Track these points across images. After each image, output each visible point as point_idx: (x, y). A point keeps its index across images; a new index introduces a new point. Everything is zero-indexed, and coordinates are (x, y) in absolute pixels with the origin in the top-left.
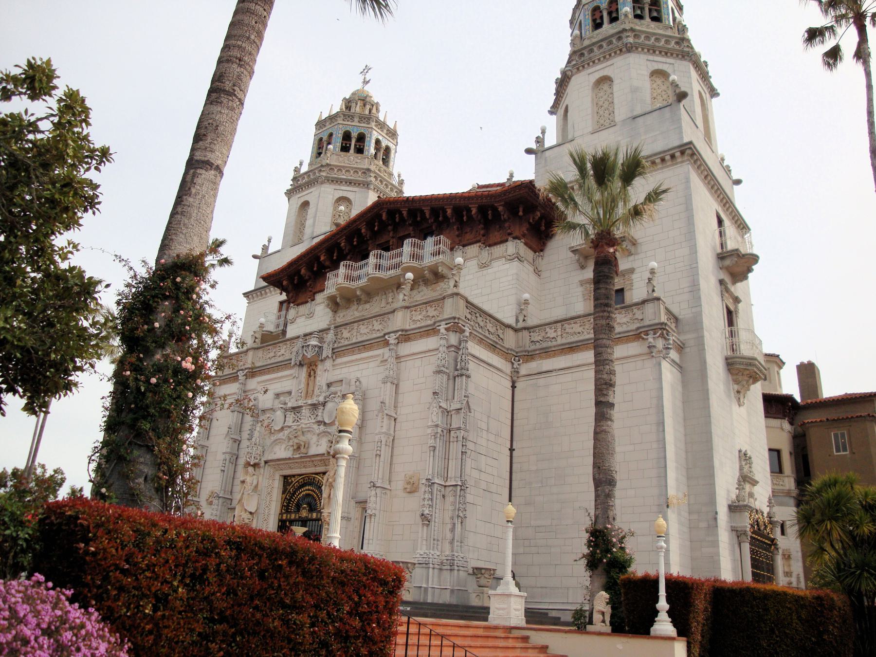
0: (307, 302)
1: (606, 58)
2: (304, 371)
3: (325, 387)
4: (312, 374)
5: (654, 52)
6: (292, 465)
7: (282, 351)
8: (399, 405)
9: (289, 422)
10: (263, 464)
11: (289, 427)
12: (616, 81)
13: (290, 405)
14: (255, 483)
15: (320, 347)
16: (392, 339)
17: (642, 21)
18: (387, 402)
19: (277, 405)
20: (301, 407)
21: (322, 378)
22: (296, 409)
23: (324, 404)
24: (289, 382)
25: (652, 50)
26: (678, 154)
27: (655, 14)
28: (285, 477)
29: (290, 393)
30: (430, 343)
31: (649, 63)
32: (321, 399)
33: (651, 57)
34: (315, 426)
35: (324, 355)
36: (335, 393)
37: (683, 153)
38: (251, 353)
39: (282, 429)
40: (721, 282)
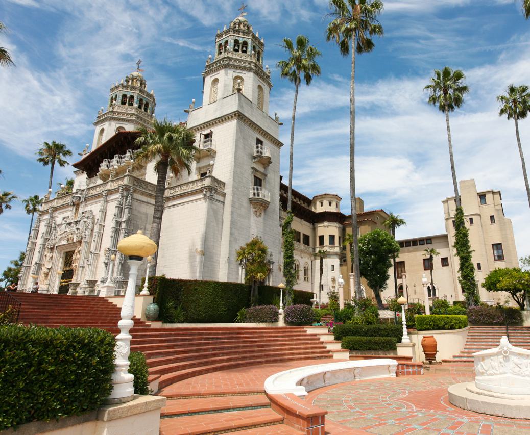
0: (93, 177)
1: (218, 69)
2: (75, 208)
3: (81, 214)
4: (77, 210)
5: (237, 68)
6: (68, 248)
7: (68, 199)
8: (106, 220)
9: (67, 229)
10: (55, 247)
11: (66, 231)
12: (219, 79)
13: (68, 222)
14: (51, 256)
15: (80, 197)
16: (104, 193)
17: (237, 53)
18: (100, 219)
19: (64, 222)
20: (71, 223)
21: (81, 210)
22: (70, 224)
23: (80, 221)
24: (69, 213)
25: (236, 67)
26: (233, 115)
27: (244, 49)
28: (67, 253)
29: (69, 217)
30: (117, 196)
31: (234, 73)
32: (79, 219)
33: (235, 71)
34: (76, 231)
35: (81, 201)
36: (84, 216)
37: (235, 115)
38: (56, 201)
39: (64, 232)
40: (253, 168)
